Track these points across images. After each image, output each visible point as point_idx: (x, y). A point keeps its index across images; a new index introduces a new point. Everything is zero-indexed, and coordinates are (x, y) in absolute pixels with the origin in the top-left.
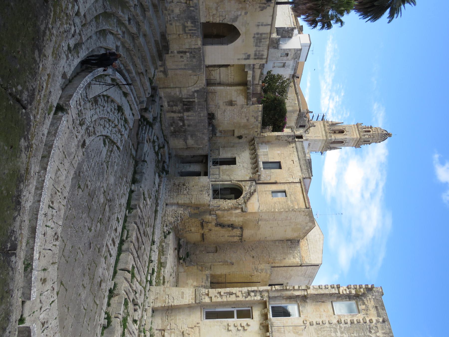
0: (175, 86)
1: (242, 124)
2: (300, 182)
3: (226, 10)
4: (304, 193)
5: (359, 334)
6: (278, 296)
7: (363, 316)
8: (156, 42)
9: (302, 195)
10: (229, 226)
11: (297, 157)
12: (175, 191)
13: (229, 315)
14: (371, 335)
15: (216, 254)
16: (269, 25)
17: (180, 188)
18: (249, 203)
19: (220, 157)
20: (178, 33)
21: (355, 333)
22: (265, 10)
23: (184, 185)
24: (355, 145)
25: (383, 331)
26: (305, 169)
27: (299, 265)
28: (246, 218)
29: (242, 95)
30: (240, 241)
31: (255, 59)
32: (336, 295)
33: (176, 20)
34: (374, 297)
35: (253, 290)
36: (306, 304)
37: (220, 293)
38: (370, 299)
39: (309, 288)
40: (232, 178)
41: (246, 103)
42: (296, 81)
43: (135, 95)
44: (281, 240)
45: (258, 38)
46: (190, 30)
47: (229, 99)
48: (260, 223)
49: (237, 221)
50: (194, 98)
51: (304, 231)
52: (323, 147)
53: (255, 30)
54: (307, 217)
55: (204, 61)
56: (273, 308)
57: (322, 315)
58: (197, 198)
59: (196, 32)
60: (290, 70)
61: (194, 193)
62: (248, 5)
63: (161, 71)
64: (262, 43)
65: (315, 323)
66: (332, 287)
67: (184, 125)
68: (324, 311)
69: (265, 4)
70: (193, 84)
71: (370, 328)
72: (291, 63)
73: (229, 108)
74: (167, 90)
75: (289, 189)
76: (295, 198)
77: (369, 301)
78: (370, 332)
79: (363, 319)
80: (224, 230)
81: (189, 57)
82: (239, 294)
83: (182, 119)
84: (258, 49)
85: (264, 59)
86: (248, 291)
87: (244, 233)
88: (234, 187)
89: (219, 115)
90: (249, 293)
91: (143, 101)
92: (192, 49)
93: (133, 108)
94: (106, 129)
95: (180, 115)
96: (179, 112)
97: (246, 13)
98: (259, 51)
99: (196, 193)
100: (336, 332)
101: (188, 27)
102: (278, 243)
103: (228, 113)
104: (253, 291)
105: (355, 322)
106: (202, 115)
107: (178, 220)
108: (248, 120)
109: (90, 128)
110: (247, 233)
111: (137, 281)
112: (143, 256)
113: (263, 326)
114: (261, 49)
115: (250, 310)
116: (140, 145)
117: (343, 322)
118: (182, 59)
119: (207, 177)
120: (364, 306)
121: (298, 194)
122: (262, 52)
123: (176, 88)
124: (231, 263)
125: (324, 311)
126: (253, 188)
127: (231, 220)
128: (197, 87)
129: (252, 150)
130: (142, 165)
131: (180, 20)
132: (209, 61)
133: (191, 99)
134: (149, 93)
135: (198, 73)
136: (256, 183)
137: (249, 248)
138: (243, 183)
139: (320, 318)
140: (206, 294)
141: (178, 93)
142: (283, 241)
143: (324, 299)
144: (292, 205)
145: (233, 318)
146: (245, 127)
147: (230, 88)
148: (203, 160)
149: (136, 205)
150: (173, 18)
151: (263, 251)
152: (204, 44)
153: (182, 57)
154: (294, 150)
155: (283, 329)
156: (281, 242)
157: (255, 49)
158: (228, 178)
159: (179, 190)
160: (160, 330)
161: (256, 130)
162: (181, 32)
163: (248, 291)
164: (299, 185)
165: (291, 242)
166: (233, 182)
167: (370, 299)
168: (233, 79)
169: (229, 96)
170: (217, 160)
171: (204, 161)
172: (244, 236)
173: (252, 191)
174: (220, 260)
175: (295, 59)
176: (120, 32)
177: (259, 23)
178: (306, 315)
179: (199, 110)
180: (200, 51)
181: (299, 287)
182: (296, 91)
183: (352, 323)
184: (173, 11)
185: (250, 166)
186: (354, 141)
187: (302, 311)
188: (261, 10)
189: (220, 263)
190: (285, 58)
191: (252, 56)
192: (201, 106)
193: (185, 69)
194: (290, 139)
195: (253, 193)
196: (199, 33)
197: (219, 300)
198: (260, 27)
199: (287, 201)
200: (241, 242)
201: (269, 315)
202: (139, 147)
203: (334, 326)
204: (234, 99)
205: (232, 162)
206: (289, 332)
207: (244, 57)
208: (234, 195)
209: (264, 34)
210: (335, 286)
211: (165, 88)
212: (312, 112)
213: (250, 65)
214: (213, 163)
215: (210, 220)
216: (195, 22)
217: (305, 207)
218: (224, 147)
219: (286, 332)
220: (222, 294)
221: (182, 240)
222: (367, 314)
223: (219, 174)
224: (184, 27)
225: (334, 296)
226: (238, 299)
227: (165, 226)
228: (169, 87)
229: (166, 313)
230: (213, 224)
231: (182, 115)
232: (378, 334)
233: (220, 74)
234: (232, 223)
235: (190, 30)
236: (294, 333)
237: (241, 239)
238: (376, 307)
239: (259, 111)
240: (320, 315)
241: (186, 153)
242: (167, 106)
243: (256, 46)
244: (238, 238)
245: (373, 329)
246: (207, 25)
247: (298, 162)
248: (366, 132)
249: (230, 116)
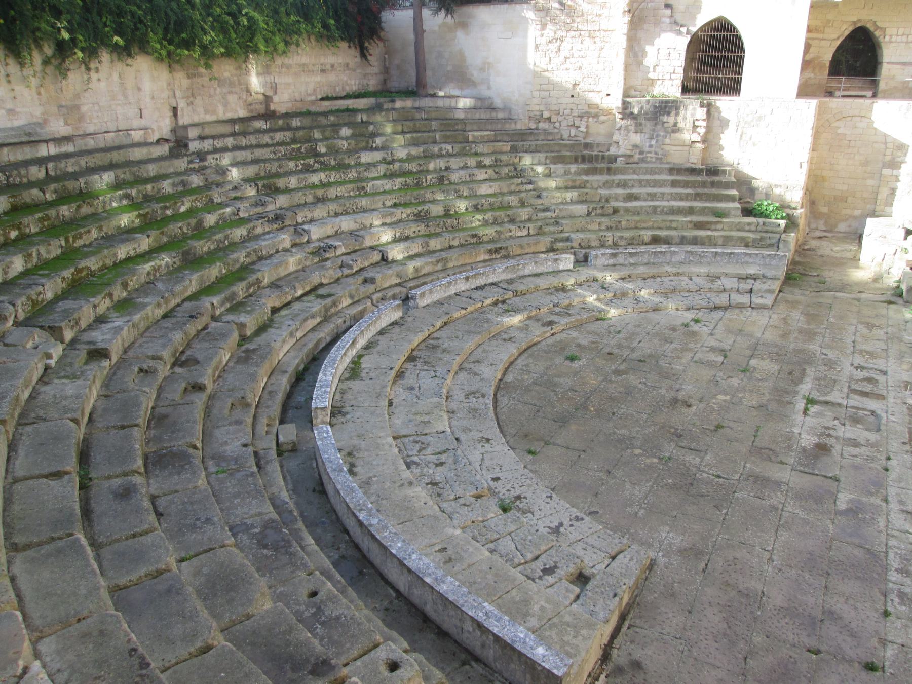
33: (657, 142)
131: (658, 136)
150: (651, 146)
184: (635, 146)
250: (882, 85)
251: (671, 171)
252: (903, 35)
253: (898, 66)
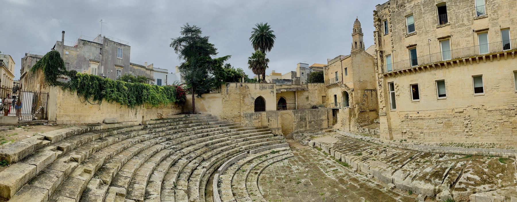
8: (258, 131)
51: (367, 56)
53: (258, 90)
67: (314, 121)
73: (310, 99)
82: (381, 90)
89: (314, 104)
96: (306, 123)
114: (268, 87)
185: (336, 88)
191: (272, 90)
197: (384, 102)
205: (335, 96)
213: (277, 91)
237: (374, 90)
244: (373, 92)
246: (256, 110)
251: (257, 128)
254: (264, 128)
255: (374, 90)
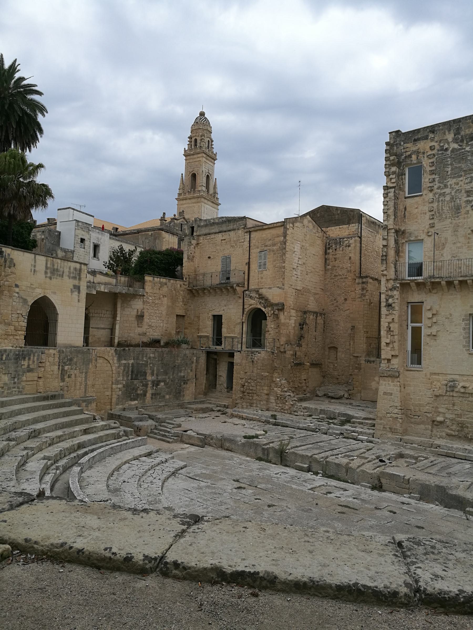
0: (110, 390)
1: (170, 304)
2: (250, 232)
3: (10, 312)
4: (264, 227)
5: (449, 165)
6: (395, 268)
7: (426, 158)
9: (268, 230)
10: (302, 329)
11: (217, 235)
12: (251, 398)
13: (416, 333)
14: (450, 149)
15: (339, 349)
16: (35, 257)
17: (248, 391)
18: (272, 301)
19: (211, 336)
20: (36, 379)
21: (447, 169)
22: (15, 261)
23: (243, 386)
24: (213, 161)
25: (447, 133)
26: (234, 225)
27: (359, 240)
28: (292, 305)
29: (130, 301)
30: (323, 316)
31: (80, 279)
32: (397, 192)
33: (18, 379)
34: (402, 143)
35: (385, 300)
36: (407, 231)
37: (387, 343)
38: (404, 149)
39: (387, 226)
40: (239, 321)
41: (142, 297)
42: (122, 233)
43: (116, 441)
44: (326, 262)
45: (51, 273)
46: (34, 362)
47: (133, 319)
48: (298, 288)
49: (296, 318)
50: (129, 364)
52: (213, 202)
53: (41, 276)
54: (296, 225)
55: (77, 347)
56: (409, 276)
57: (422, 211)
58: (262, 368)
59: (36, 355)
60: (103, 237)
61: (255, 371)
62: (6, 283)
63: (87, 406)
64: (59, 268)
65: (432, 221)
66: (386, 195)
67: (164, 381)
68: (417, 208)
69: (5, 261)
70: (109, 365)
71: (442, 150)
72: (94, 237)
73: (146, 319)
74: (114, 400)
75: (258, 248)
76: (270, 240)
77: (407, 150)
78: (447, 150)
79: (430, 159)
80: (306, 336)
81: (70, 367)
83: (156, 383)
84: (68, 274)
85: (81, 267)
86: (385, 306)
87: (312, 310)
88: (250, 319)
89: (155, 334)
90: (389, 306)
91: (124, 431)
92: (59, 362)
93: (132, 445)
94: (154, 481)
95: (150, 385)
96: (146, 385)
97: (17, 286)
98: (70, 272)
99: (255, 369)
100: (444, 194)
101: (29, 366)
102: (329, 265)
103: (152, 321)
104: (387, 300)
105: (433, 168)
106: (152, 355)
107: (289, 396)
108: (164, 296)
109: (150, 500)
110: (312, 306)
111: (364, 453)
112: (332, 444)
113: (433, 289)
114: (66, 270)
115: (411, 306)
116: (184, 440)
117: (431, 185)
118: (73, 376)
119: (235, 354)
120: (413, 156)
121: (265, 235)
122: (72, 269)
123: (112, 388)
124: (352, 329)
125: (417, 208)
126: (254, 295)
127: (293, 325)
128: (113, 360)
129: (204, 293)
130: (212, 439)
131: (18, 375)
132: (80, 341)
133: (129, 369)
134: (115, 423)
135: (94, 356)
136: (248, 290)
137: (333, 304)
138: (245, 307)
139: (426, 214)
140: (388, 362)
141: (120, 386)
142: (326, 259)
143: (401, 207)
144: (279, 244)
145: (420, 328)
146: (174, 300)
147: (118, 315)
148: (212, 358)
149: (263, 449)
150: (15, 383)
151: (338, 286)
152: (55, 345)
153: (69, 377)
154: (208, 238)
155: (438, 264)
156: (328, 261)
157: (67, 278)
158: (239, 327)
159: (251, 392)
160: (432, 427)
161: (179, 286)
162: (36, 374)
163: (385, 306)
164: (253, 235)
165: (329, 248)
166: (243, 321)
167: (404, 149)
168: (107, 311)
169: (130, 319)
170: (215, 340)
171: (215, 357)
172: (316, 310)
173: (257, 296)
174: (348, 343)
175: (89, 230)
176: (25, 453)
177: (31, 270)
178: (421, 232)
179: (145, 359)
180: (63, 351)
181: (384, 239)
182: (135, 233)
183: (432, 172)
184: (5, 384)
186: (207, 161)
187: (416, 237)
188: (14, 265)
189: (352, 344)
190: (87, 243)
191: (76, 282)
192: (140, 356)
193: (86, 373)
194: (194, 242)
195: (259, 295)
196: (37, 350)
197: (396, 345)
198: (37, 269)
199: (273, 251)
200: (324, 314)
201: (419, 281)
202: (187, 441)
203: (437, 196)
204: (134, 313)
205: (218, 320)
206: (442, 255)
207: (76, 293)
208: (263, 321)
209: (47, 264)
210: (386, 191)
211: (111, 402)
212: (164, 214)
213: (88, 287)
214: (218, 345)
215: (291, 352)
216: (23, 354)
217: (283, 227)
218: (198, 329)
219: (441, 259)
220: (388, 341)
221: (318, 392)
222: (424, 153)
223: (233, 338)
224: (30, 370)
225: (399, 194)
226: (396, 320)
227: (296, 413)
228: (110, 397)
229: (412, 418)
230: (297, 349)
231: (150, 383)
232: (450, 140)
233: (98, 328)
234: (298, 325)
235: (34, 362)
236: (443, 249)
237: (321, 314)
238: (415, 140)
239: (154, 280)
240: (421, 214)
241: (203, 380)
242: (136, 402)
243: (62, 277)
244: (319, 318)
245: (443, 146)
247: (223, 234)
248: (196, 145)
249: (158, 319)
250: (90, 340)
252: (97, 313)
253: (96, 330)
254: (53, 397)
255: (321, 314)
